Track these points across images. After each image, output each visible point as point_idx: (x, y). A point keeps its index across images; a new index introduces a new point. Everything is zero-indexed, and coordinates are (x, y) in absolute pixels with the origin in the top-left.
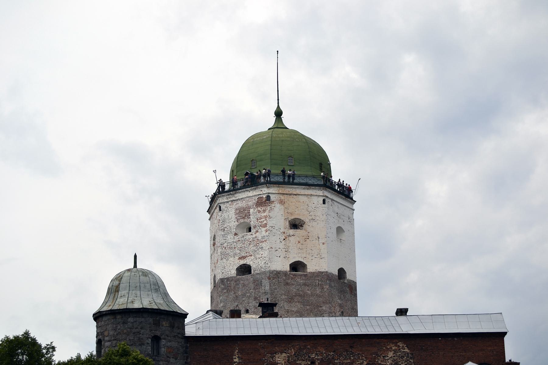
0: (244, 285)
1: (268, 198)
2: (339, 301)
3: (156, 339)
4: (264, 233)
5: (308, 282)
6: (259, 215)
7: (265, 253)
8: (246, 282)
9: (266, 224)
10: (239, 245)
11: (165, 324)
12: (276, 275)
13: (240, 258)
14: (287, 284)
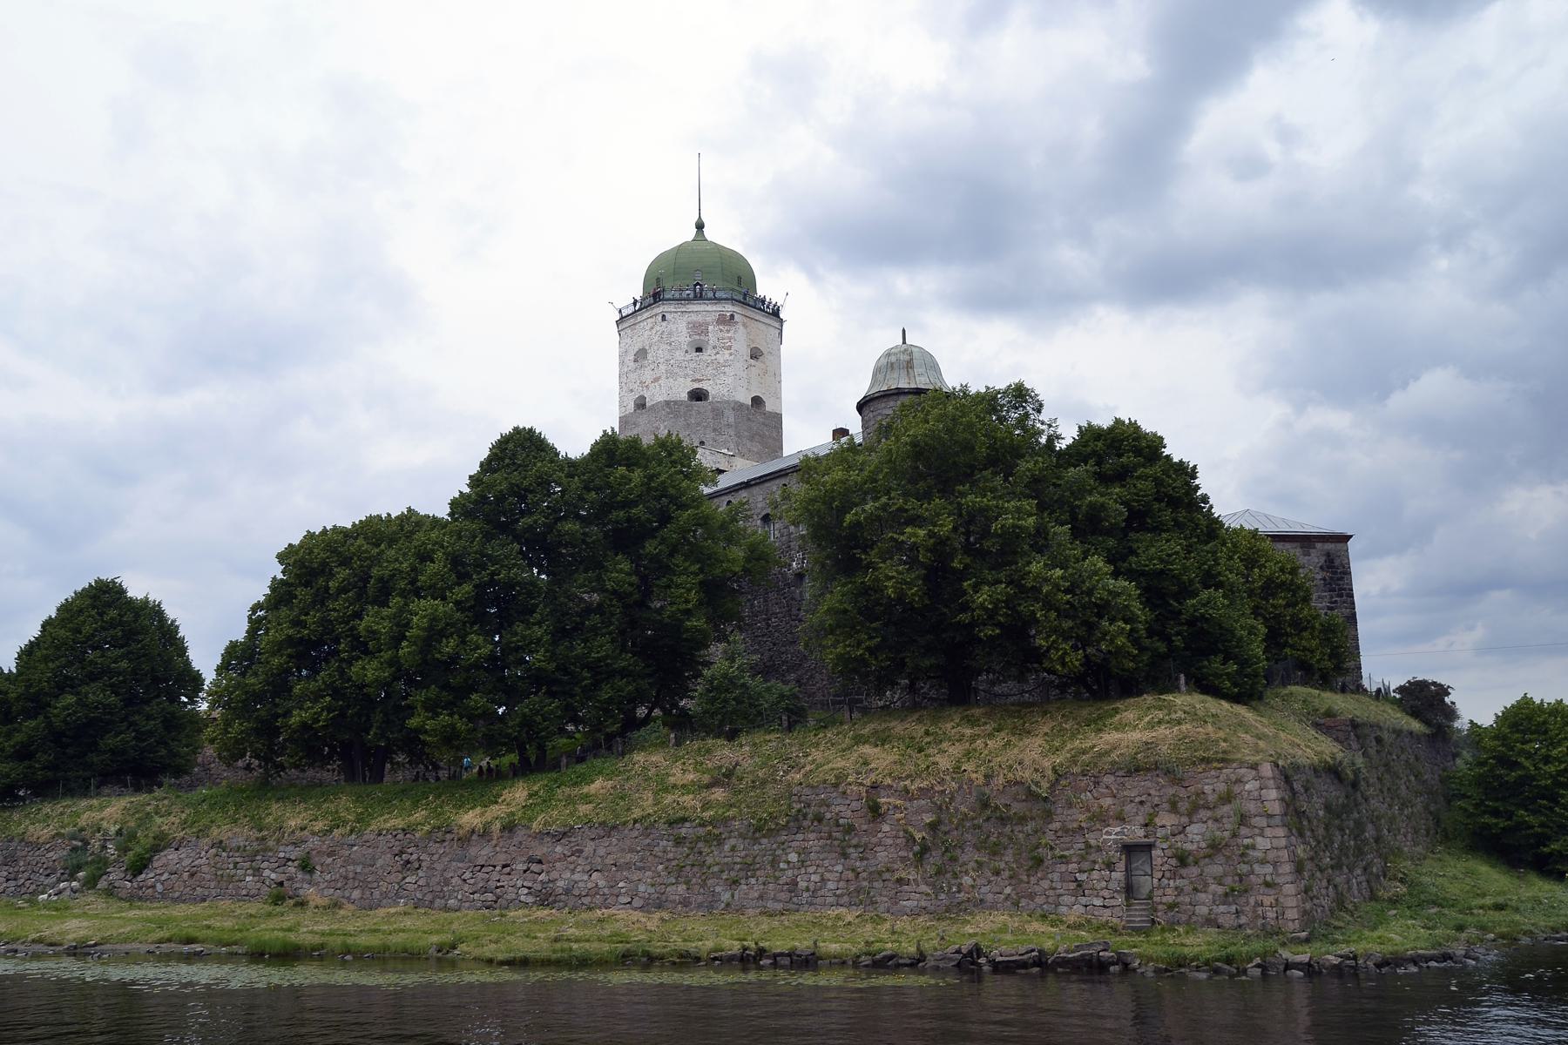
0: (699, 413)
1: (732, 317)
4: (727, 357)
5: (767, 422)
6: (721, 335)
7: (729, 380)
8: (702, 410)
9: (731, 347)
10: (692, 365)
12: (739, 407)
13: (693, 381)
14: (749, 419)
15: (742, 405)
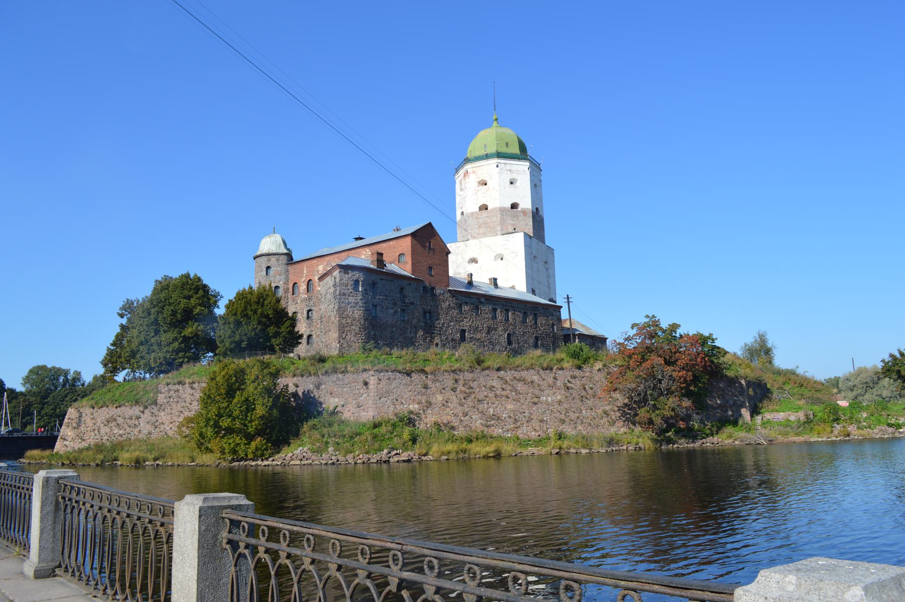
2: (512, 222)
3: (268, 268)
11: (273, 259)
14: (478, 218)
15: (472, 214)
